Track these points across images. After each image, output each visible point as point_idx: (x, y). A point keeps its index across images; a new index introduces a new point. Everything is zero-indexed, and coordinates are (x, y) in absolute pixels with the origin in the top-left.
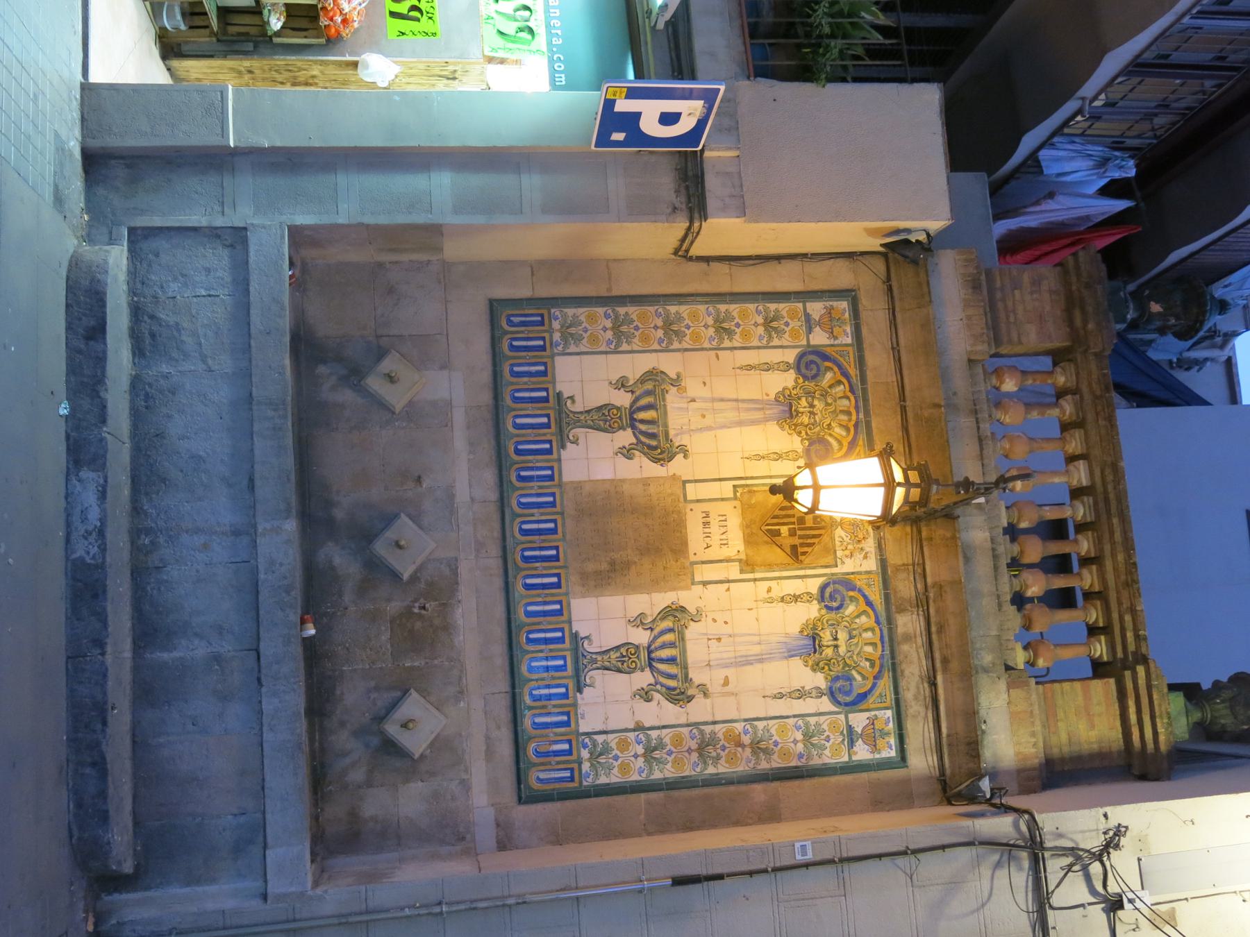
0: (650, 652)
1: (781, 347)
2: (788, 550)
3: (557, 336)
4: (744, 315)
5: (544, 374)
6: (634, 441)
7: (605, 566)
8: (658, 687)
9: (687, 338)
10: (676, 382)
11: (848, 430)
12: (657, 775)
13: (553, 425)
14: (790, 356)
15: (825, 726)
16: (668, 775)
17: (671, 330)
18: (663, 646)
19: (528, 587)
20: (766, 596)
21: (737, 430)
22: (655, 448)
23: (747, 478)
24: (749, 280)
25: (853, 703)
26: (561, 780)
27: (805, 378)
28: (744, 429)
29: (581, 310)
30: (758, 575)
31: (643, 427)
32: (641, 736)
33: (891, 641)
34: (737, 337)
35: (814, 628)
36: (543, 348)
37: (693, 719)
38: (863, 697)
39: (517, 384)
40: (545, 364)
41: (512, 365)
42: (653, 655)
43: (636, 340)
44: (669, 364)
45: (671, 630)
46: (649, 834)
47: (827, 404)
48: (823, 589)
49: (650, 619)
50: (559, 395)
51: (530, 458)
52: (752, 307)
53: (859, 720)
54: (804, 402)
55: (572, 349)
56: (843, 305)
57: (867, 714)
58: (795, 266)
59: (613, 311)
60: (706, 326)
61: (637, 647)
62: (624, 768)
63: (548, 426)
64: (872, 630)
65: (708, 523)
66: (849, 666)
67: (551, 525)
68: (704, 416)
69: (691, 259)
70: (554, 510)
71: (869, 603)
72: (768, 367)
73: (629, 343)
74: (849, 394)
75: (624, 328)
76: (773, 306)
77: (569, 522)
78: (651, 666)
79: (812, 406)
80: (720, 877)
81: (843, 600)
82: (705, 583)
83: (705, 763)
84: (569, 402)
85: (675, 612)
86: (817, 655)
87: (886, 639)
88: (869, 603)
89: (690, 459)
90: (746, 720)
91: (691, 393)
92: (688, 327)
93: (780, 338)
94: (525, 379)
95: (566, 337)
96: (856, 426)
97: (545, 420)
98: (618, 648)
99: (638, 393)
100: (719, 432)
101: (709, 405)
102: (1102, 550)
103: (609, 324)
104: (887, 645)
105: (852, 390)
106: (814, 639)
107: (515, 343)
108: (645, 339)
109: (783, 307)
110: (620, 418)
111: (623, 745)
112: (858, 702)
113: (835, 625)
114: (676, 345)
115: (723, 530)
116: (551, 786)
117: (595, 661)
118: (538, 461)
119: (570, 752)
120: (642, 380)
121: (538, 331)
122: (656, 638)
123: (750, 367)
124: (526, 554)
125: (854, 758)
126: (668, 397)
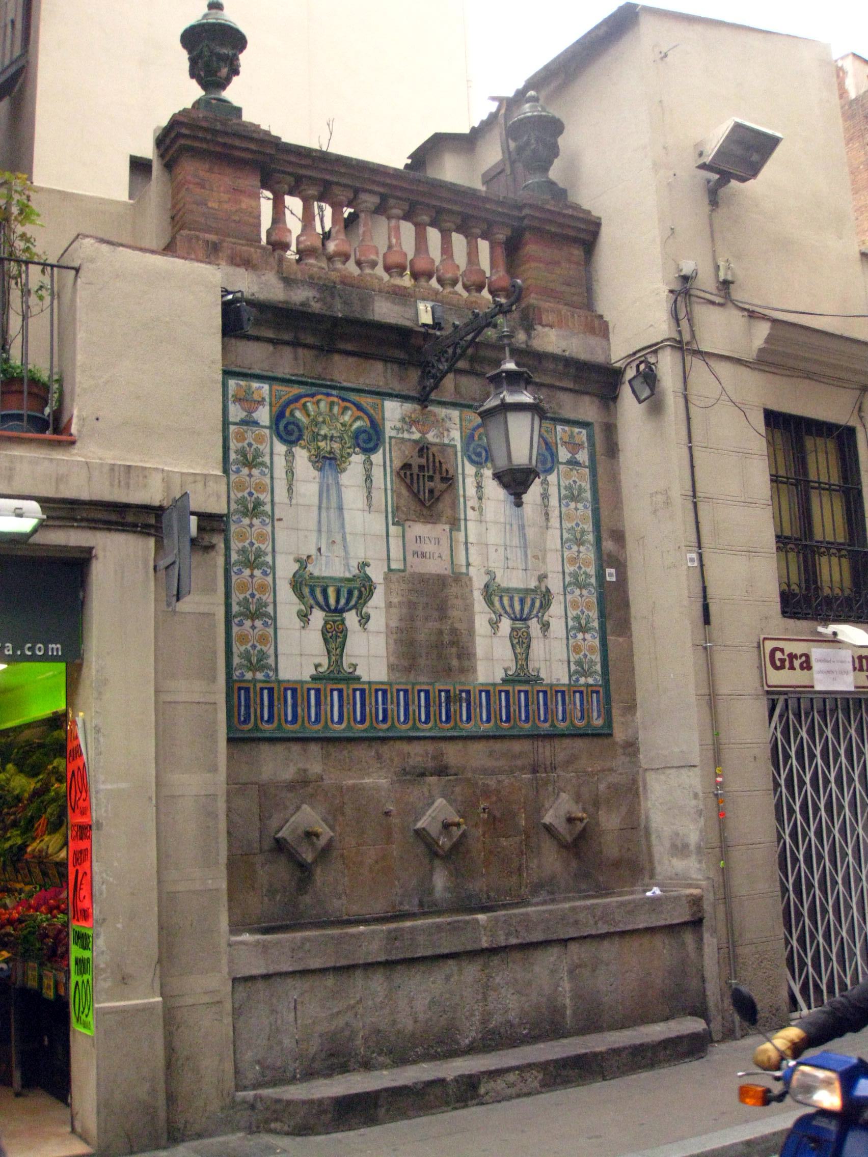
1: (272, 454)
2: (444, 486)
3: (260, 676)
6: (354, 611)
7: (454, 650)
9: (263, 547)
10: (303, 563)
11: (346, 409)
12: (596, 624)
13: (340, 686)
14: (280, 448)
17: (253, 561)
19: (469, 719)
20: (477, 513)
21: (346, 513)
22: (360, 592)
26: (598, 701)
27: (300, 438)
28: (345, 507)
30: (462, 517)
31: (343, 601)
34: (262, 497)
39: (303, 717)
40: (286, 689)
42: (518, 616)
43: (264, 598)
44: (286, 568)
45: (501, 598)
47: (324, 422)
48: (472, 462)
49: (493, 616)
50: (314, 678)
53: (563, 454)
54: (322, 444)
55: (271, 661)
57: (559, 446)
59: (235, 617)
60: (251, 526)
61: (513, 629)
62: (591, 649)
63: (340, 692)
65: (422, 553)
67: (422, 694)
68: (334, 542)
70: (410, 692)
72: (290, 472)
73: (266, 605)
74: (315, 399)
75: (253, 608)
77: (422, 679)
78: (526, 619)
79: (325, 437)
80: (704, 589)
81: (479, 445)
84: (320, 669)
85: (489, 592)
89: (371, 561)
90: (562, 547)
91: (313, 552)
94: (299, 710)
95: (262, 668)
96: (344, 400)
97: (335, 693)
98: (513, 645)
99: (312, 602)
100: (348, 529)
101: (324, 535)
102: (434, 206)
103: (248, 623)
107: (266, 717)
108: (262, 588)
110: (334, 622)
111: (577, 649)
114: (269, 559)
116: (602, 710)
117: (522, 666)
118: (371, 704)
119: (581, 692)
120: (301, 597)
121: (255, 692)
122: (506, 612)
123: (290, 489)
124: (444, 718)
125: (587, 464)
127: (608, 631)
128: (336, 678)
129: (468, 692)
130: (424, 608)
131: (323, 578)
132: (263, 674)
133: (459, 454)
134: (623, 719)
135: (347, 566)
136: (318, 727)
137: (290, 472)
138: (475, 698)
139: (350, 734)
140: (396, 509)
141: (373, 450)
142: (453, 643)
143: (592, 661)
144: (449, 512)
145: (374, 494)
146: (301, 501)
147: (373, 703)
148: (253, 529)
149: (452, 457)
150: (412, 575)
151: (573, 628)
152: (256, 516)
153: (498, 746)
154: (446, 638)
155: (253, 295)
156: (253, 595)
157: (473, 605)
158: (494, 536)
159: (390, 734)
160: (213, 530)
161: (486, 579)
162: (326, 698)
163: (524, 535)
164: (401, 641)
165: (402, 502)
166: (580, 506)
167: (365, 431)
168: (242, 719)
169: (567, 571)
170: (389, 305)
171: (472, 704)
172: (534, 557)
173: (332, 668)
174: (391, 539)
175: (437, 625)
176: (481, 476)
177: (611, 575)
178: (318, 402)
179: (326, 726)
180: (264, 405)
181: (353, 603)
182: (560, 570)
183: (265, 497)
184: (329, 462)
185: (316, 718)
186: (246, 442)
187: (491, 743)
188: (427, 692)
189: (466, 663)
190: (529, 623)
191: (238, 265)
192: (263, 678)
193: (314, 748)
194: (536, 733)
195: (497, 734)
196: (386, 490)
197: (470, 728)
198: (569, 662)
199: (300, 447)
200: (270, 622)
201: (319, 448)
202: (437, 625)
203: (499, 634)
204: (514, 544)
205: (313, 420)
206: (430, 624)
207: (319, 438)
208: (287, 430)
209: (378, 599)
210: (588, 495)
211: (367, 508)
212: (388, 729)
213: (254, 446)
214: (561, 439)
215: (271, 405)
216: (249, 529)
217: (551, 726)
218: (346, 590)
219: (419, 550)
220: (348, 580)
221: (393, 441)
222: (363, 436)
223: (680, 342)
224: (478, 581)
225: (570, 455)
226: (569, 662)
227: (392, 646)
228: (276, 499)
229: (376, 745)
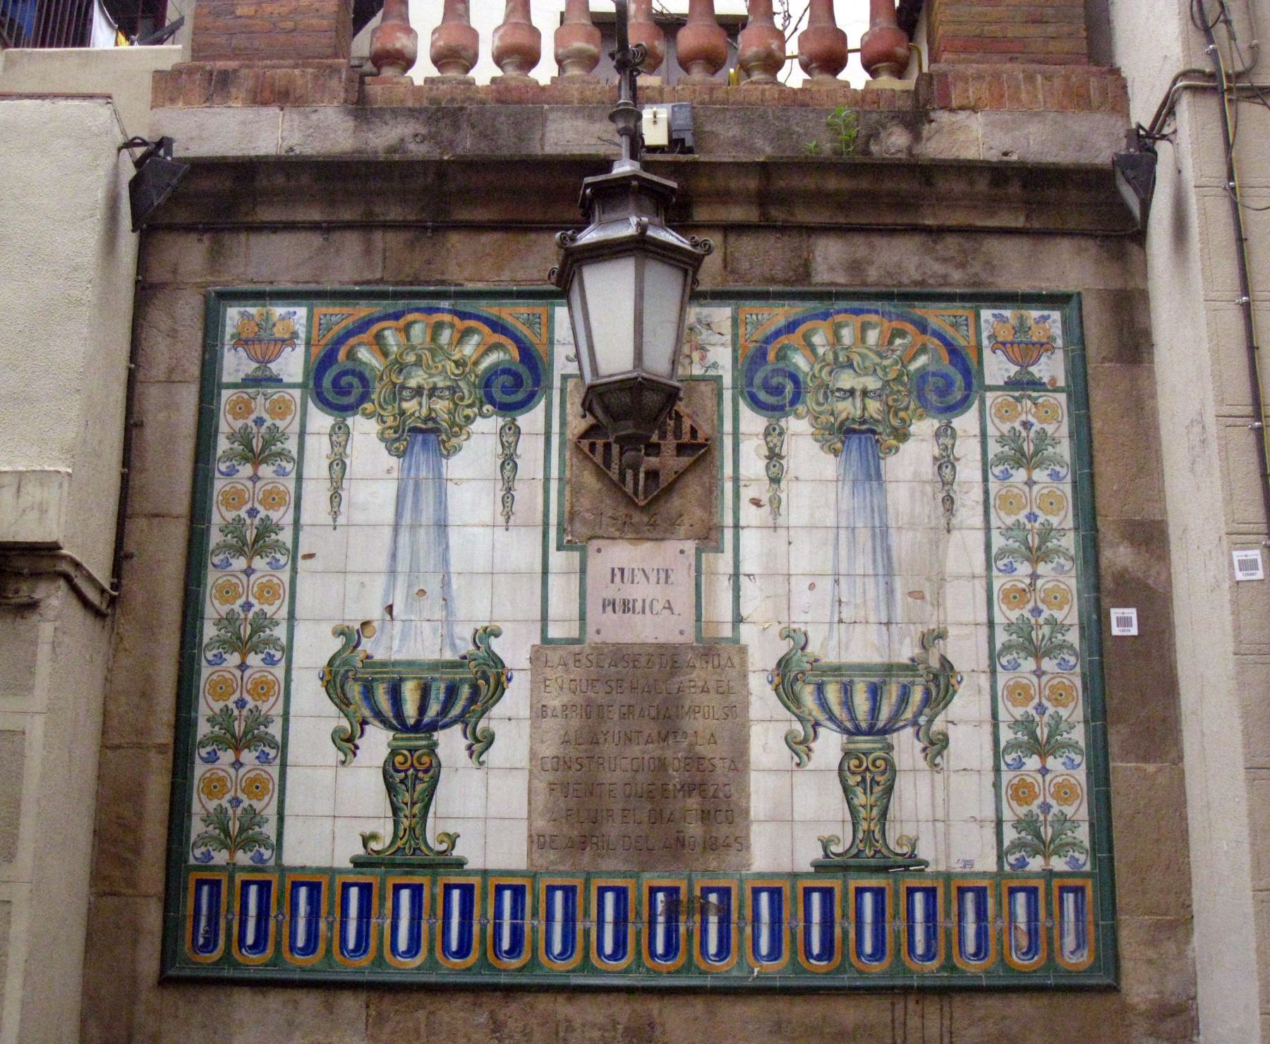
0: (858, 731)
1: (302, 434)
2: (685, 461)
3: (243, 858)
4: (234, 499)
5: (314, 888)
6: (458, 728)
7: (693, 802)
8: (922, 720)
9: (270, 610)
10: (352, 637)
11: (467, 332)
12: (1078, 735)
13: (416, 880)
14: (320, 421)
15: (1005, 428)
16: (1079, 714)
17: (248, 638)
18: (848, 703)
21: (454, 536)
22: (475, 690)
23: (546, 525)
24: (170, 480)
25: (966, 373)
27: (364, 397)
28: (452, 519)
29: (196, 807)
30: (728, 520)
31: (434, 709)
32: (1009, 759)
33: (859, 296)
34: (275, 516)
35: (830, 429)
36: (264, 887)
37: (984, 663)
38: (954, 352)
41: (292, 948)
42: (864, 725)
43: (264, 708)
44: (314, 647)
45: (820, 688)
46: (1181, 758)
47: (418, 363)
49: (798, 726)
50: (358, 863)
51: (476, 929)
52: (219, 484)
53: (997, 368)
56: (233, 314)
57: (987, 353)
58: (152, 396)
61: (847, 754)
62: (1065, 793)
63: (417, 891)
64: (837, 328)
65: (625, 603)
66: (900, 376)
67: (610, 898)
68: (422, 592)
69: (115, 587)
71: (791, 327)
72: (338, 464)
73: (267, 721)
74: (402, 322)
75: (239, 727)
76: (223, 445)
78: (885, 731)
79: (418, 391)
82: (738, 620)
83: (1061, 647)
84: (374, 845)
85: (786, 679)
86: (880, 429)
87: (856, 304)
88: (791, 327)
90: (989, 567)
91: (375, 612)
92: (247, 606)
93: (284, 436)
94: (323, 925)
95: (247, 840)
96: (463, 316)
97: (405, 895)
98: (847, 790)
99: (367, 713)
100: (455, 566)
101: (401, 581)
103: (227, 757)
104: (866, 305)
105: (397, 316)
106: (854, 431)
107: (250, 939)
108: (262, 689)
109: (226, 424)
111: (1022, 792)
112: (965, 364)
113: (828, 391)
114: (280, 632)
115: (639, 576)
117: (869, 833)
118: (484, 915)
119: (1032, 892)
120: (342, 702)
123: (335, 496)
124: (660, 949)
125: (1061, 383)
126: (379, 656)
127: (1114, 748)
128: (410, 862)
129: (725, 893)
130: (623, 716)
131: (395, 664)
132: (250, 854)
133: (728, 395)
134: (1151, 953)
135: (449, 639)
136: (364, 961)
137: (338, 464)
139: (433, 979)
140: (569, 518)
141: (525, 404)
142: (689, 789)
143: (1063, 819)
145: (520, 491)
146: (359, 517)
148: (253, 578)
149: (710, 404)
150: (599, 649)
151: (1012, 746)
152: (259, 553)
153: (799, 1010)
154: (676, 777)
155: (292, 149)
156: (241, 703)
157: (746, 705)
158: (807, 556)
159: (524, 980)
160: (37, 575)
161: (783, 647)
162: (382, 905)
163: (888, 550)
164: (565, 786)
165: (585, 503)
166: (1040, 475)
167: (506, 371)
168: (201, 941)
169: (999, 618)
170: (580, 124)
171: (734, 916)
172: (911, 594)
173: (399, 843)
174: (551, 578)
175: (653, 750)
176: (781, 434)
177: (1124, 622)
178: (407, 329)
179: (379, 960)
180: (294, 346)
181: (456, 710)
182: (982, 617)
183: (283, 516)
184: (422, 438)
185: (308, 940)
186: (253, 416)
187: (781, 1005)
188: (621, 893)
189: (723, 831)
190: (894, 738)
191: (265, 103)
192: (251, 863)
193: (350, 1004)
194: (899, 982)
195: (794, 983)
196: (547, 479)
197: (729, 970)
198: (999, 823)
199: (364, 414)
200: (272, 753)
201: (402, 413)
202: (653, 750)
203: (811, 766)
204: (860, 571)
205: (397, 361)
206: (636, 750)
207: (406, 393)
208: (336, 386)
209: (516, 700)
210: (1064, 450)
212: (521, 970)
213: (269, 423)
214: (992, 337)
215: (308, 344)
216: (243, 577)
217: (942, 968)
218: (443, 686)
219: (619, 598)
220: (452, 665)
221: (571, 384)
222: (507, 380)
223: (1212, 76)
224: (762, 651)
225: (1014, 369)
226: (999, 823)
227: (541, 800)
228: (305, 518)
229: (491, 1002)
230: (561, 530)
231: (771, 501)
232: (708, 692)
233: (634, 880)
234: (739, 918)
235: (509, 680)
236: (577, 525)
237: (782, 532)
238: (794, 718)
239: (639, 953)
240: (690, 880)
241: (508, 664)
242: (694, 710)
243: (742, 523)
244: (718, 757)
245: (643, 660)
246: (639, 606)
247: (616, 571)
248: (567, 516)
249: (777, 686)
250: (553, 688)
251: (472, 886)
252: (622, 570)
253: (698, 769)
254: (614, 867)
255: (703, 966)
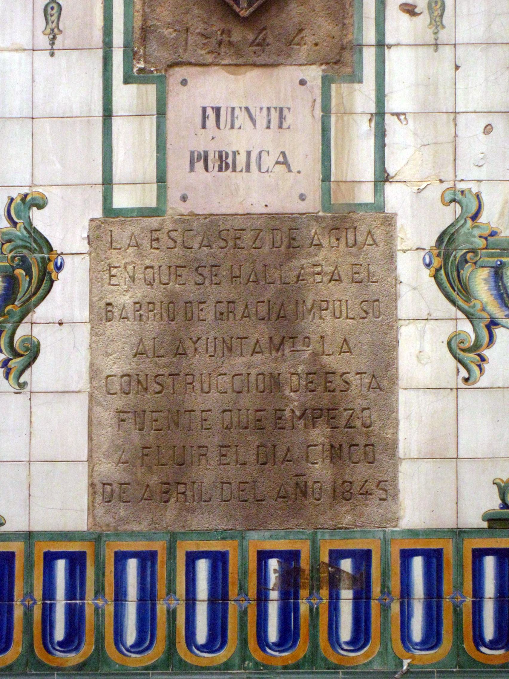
7: (319, 434)
20: (424, 20)
23: (108, 46)
30: (369, 35)
49: (466, 327)
65: (222, 157)
67: (203, 567)
70: (161, 558)
82: (382, 178)
85: (450, 261)
115: (242, 118)
118: (29, 594)
124: (273, 635)
129: (363, 558)
130: (220, 316)
138: (385, 574)
140: (141, 36)
142: (312, 415)
144: (323, 27)
147: (38, 593)
150: (186, 222)
154: (294, 401)
157: (394, 298)
161: (447, 216)
164: (139, 414)
171: (376, 589)
174: (117, 124)
175: (263, 363)
188: (219, 561)
189: (359, 473)
202: (263, 363)
203: (484, 381)
206: (238, 363)
209: (69, 296)
211: (43, 41)
219: (213, 148)
224: (417, 223)
227: (107, 434)
230: (130, 55)
231: (430, 7)
232: (340, 280)
233: (236, 543)
234: (382, 592)
235: (59, 268)
236: (153, 46)
237: (447, 52)
238: (460, 315)
239: (244, 642)
240: (314, 542)
241: (56, 246)
242: (322, 306)
243: (389, 40)
244: (353, 369)
245: (248, 237)
246: (241, 160)
247: (209, 112)
248: (137, 34)
249: (438, 270)
250: (122, 278)
251: (13, 554)
252: (217, 111)
253: (326, 389)
254: (208, 525)
255: (333, 659)
